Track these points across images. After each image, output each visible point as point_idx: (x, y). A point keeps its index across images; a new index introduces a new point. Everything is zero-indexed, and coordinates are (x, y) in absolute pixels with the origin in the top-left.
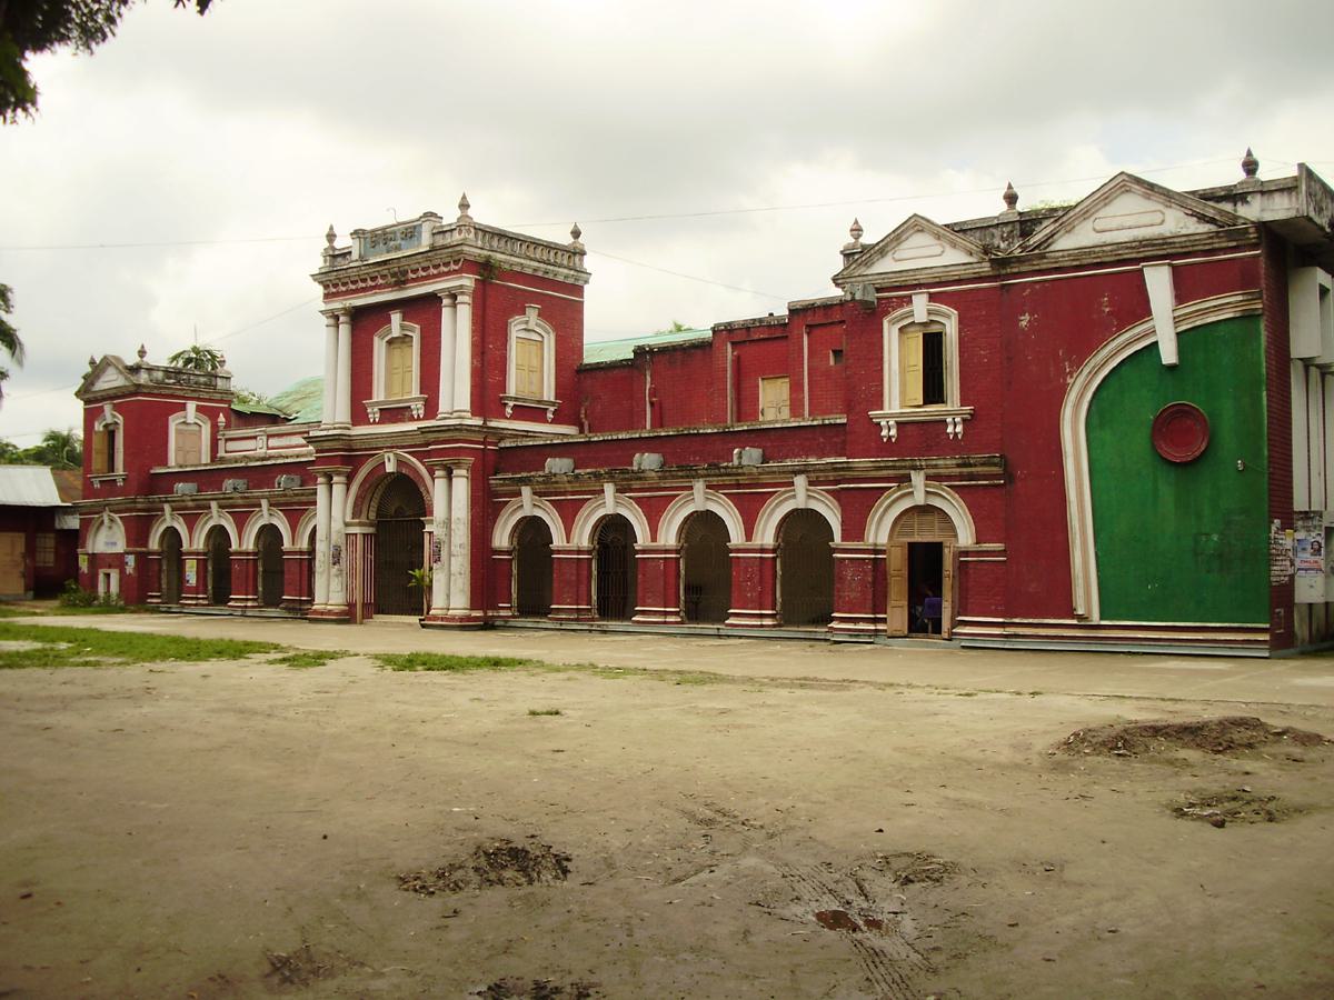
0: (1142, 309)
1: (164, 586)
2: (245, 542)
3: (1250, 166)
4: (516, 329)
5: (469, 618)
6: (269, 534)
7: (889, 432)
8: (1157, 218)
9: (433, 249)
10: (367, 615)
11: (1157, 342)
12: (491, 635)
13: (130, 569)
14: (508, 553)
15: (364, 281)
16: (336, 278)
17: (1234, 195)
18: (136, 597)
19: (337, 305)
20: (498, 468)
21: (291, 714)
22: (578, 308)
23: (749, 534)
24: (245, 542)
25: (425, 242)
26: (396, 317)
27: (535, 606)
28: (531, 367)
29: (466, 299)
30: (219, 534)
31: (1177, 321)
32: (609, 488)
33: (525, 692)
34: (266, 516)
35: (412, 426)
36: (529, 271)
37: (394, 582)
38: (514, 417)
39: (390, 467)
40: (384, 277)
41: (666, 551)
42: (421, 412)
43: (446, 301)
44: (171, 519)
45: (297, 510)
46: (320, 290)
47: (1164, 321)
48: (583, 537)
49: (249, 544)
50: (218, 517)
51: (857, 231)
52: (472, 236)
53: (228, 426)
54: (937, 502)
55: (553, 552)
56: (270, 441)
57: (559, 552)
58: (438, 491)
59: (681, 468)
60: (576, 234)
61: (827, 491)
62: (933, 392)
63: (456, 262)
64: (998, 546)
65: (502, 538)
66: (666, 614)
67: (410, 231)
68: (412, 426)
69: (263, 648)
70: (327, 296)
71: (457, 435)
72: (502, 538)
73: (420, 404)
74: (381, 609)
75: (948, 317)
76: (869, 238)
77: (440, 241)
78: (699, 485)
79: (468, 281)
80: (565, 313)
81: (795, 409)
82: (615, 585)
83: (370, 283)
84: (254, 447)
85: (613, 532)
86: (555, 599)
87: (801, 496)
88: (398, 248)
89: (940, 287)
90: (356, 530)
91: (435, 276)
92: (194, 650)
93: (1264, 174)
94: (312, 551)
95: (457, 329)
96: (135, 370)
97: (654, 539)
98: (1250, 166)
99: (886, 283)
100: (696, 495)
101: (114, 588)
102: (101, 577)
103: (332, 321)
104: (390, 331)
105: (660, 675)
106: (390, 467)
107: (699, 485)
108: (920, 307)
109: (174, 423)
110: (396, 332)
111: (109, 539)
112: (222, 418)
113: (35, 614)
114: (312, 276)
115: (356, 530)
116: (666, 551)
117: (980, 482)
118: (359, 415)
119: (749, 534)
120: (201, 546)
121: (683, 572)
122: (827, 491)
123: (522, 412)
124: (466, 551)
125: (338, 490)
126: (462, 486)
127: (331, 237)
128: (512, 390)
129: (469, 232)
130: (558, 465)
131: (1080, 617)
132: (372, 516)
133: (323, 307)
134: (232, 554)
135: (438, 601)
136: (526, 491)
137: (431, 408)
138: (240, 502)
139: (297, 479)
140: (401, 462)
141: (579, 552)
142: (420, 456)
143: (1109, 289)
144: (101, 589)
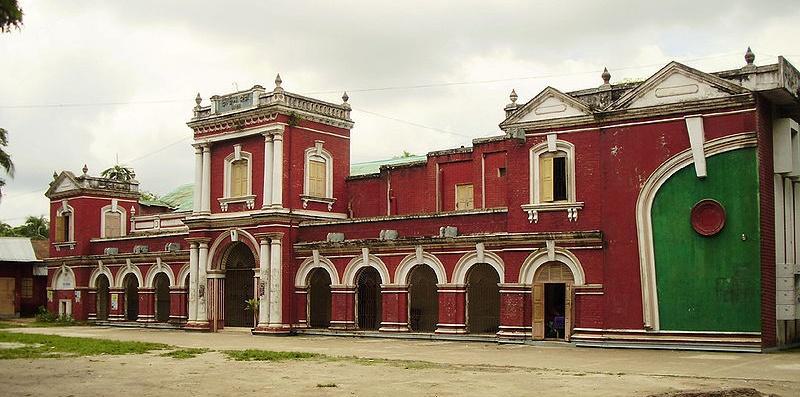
0: (684, 143)
1: (99, 310)
2: (147, 283)
3: (750, 58)
4: (309, 156)
5: (281, 329)
6: (162, 279)
7: (533, 217)
8: (694, 89)
9: (260, 107)
10: (220, 327)
11: (693, 164)
12: (295, 339)
13: (78, 300)
14: (304, 290)
15: (218, 126)
16: (201, 124)
17: (739, 75)
18: (81, 317)
19: (202, 141)
20: (299, 239)
21: (175, 386)
22: (347, 143)
24: (147, 283)
25: (255, 103)
26: (237, 148)
27: (320, 322)
28: (318, 178)
29: (280, 137)
30: (131, 278)
31: (706, 151)
32: (365, 251)
33: (317, 373)
34: (160, 267)
35: (248, 214)
36: (318, 121)
37: (237, 308)
38: (307, 208)
39: (234, 239)
40: (230, 124)
43: (267, 139)
44: (102, 270)
45: (178, 264)
46: (191, 132)
47: (698, 151)
48: (349, 280)
49: (150, 285)
50: (131, 268)
51: (514, 96)
52: (283, 99)
53: (136, 214)
54: (562, 260)
57: (335, 289)
58: (262, 253)
59: (408, 239)
60: (346, 98)
61: (496, 253)
62: (560, 192)
63: (273, 116)
64: (600, 286)
65: (301, 281)
66: (399, 326)
67: (246, 97)
68: (248, 214)
69: (157, 347)
70: (195, 136)
71: (274, 219)
72: (301, 281)
73: (252, 201)
74: (228, 325)
75: (569, 148)
76: (521, 101)
77: (264, 103)
78: (419, 249)
79: (281, 127)
80: (339, 146)
81: (477, 204)
82: (369, 309)
83: (222, 128)
84: (152, 226)
85: (368, 276)
86: (333, 317)
87: (480, 255)
88: (239, 107)
89: (564, 131)
90: (214, 276)
91: (261, 124)
92: (116, 348)
93: (758, 62)
94: (187, 289)
95: (274, 157)
96: (81, 180)
97: (392, 282)
98: (750, 58)
99: (531, 128)
101: (69, 311)
102: (61, 304)
103: (199, 151)
105: (396, 363)
106: (234, 239)
107: (419, 249)
108: (552, 142)
109: (104, 212)
110: (238, 157)
111: (66, 281)
112: (133, 209)
113: (21, 326)
115: (214, 276)
116: (399, 289)
118: (215, 207)
120: (151, 286)
121: (409, 301)
122: (496, 253)
123: (313, 206)
124: (280, 288)
125: (203, 252)
126: (277, 249)
127: (199, 100)
128: (307, 193)
129: (281, 97)
130: (335, 237)
131: (648, 328)
132: (223, 267)
135: (263, 319)
136: (315, 253)
137: (259, 203)
138: (144, 259)
139: (178, 245)
140: (240, 236)
141: (347, 289)
142: (251, 231)
143: (666, 131)
144: (61, 312)
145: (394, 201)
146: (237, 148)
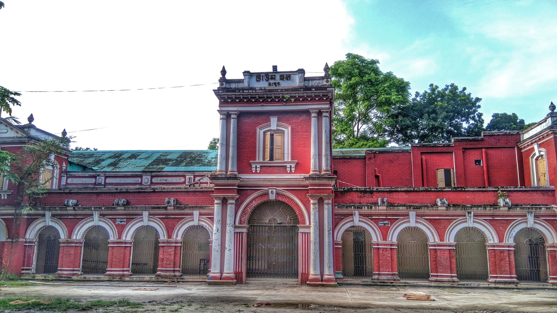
19: (234, 109)
23: (170, 236)
26: (274, 120)
41: (449, 246)
42: (293, 169)
43: (313, 115)
56: (140, 181)
61: (159, 218)
67: (287, 76)
73: (293, 166)
100: (411, 220)
104: (270, 126)
106: (272, 197)
114: (214, 90)
119: (170, 236)
122: (159, 218)
125: (230, 209)
127: (224, 72)
133: (219, 109)
134: (109, 243)
140: (278, 194)
146: (274, 120)
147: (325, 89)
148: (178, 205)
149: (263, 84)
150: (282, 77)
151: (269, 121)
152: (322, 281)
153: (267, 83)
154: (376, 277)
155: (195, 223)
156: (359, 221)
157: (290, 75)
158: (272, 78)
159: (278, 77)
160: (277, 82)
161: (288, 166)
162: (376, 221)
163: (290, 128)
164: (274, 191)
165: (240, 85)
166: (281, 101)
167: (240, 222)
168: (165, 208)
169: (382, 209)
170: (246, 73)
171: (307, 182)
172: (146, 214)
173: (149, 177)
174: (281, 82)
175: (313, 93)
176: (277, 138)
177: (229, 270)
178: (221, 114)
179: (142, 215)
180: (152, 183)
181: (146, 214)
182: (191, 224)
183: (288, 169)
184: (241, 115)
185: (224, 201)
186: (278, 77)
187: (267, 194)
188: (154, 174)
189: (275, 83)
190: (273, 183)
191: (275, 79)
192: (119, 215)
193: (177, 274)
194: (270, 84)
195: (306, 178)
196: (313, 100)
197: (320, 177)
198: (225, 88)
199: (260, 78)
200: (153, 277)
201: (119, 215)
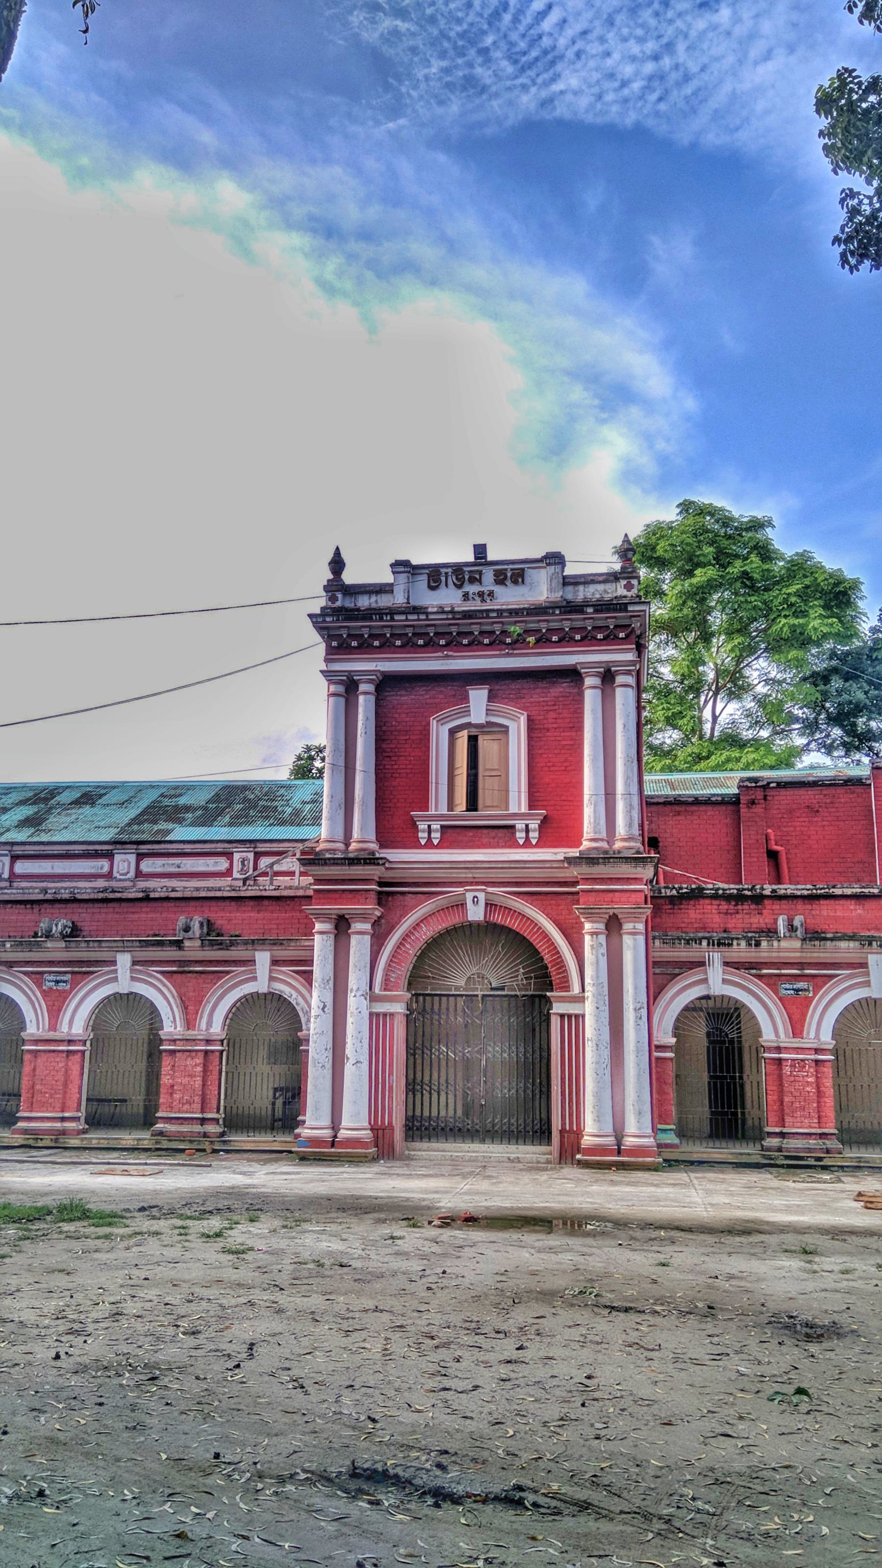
23: (190, 1024)
26: (478, 697)
42: (534, 836)
43: (589, 681)
55: (24, 1042)
56: (106, 869)
67: (513, 574)
70: (330, 651)
73: (534, 825)
104: (467, 712)
106: (476, 913)
114: (310, 616)
117: (783, 971)
125: (359, 946)
127: (337, 564)
134: (24, 1042)
137: (558, 826)
140: (490, 906)
145: (783, 858)
146: (478, 697)
147: (623, 607)
148: (213, 935)
149: (448, 597)
150: (501, 578)
151: (466, 699)
152: (619, 1152)
153: (459, 593)
154: (774, 1142)
155: (261, 985)
156: (724, 981)
157: (523, 570)
158: (472, 580)
159: (488, 575)
160: (485, 589)
161: (520, 825)
162: (772, 982)
163: (523, 720)
164: (482, 896)
165: (384, 601)
166: (498, 642)
167: (386, 986)
168: (178, 944)
169: (789, 947)
170: (401, 566)
171: (574, 872)
172: (124, 960)
173: (132, 858)
174: (498, 589)
175: (589, 620)
176: (487, 746)
177: (355, 1121)
178: (331, 682)
179: (114, 963)
180: (139, 874)
181: (124, 960)
182: (249, 988)
183: (518, 835)
184: (386, 683)
185: (342, 926)
186: (488, 575)
187: (461, 906)
188: (144, 849)
189: (481, 594)
190: (480, 875)
191: (480, 581)
192: (51, 963)
193: (212, 1129)
194: (466, 597)
195: (569, 860)
196: (588, 639)
197: (608, 858)
198: (342, 609)
199: (438, 581)
200: (144, 1137)
201: (51, 963)
